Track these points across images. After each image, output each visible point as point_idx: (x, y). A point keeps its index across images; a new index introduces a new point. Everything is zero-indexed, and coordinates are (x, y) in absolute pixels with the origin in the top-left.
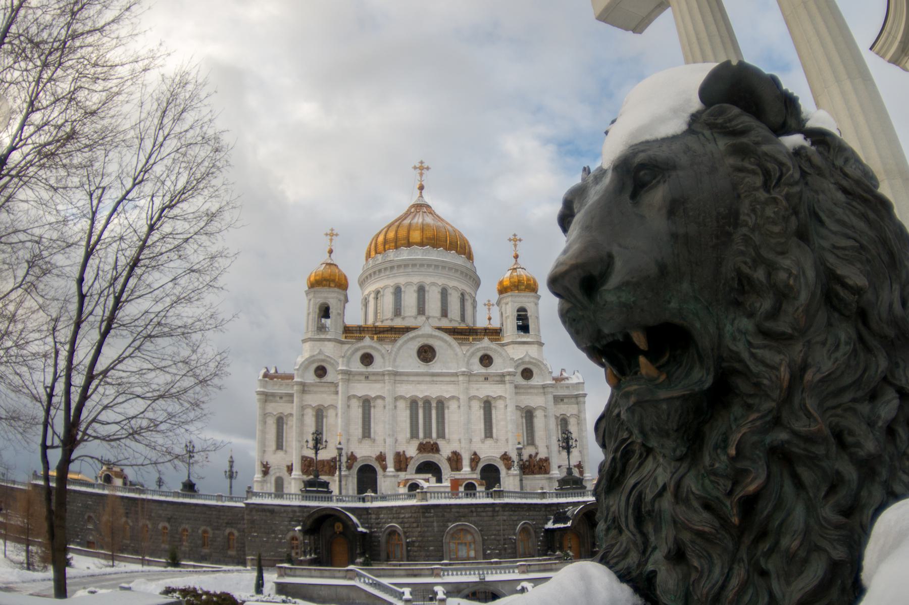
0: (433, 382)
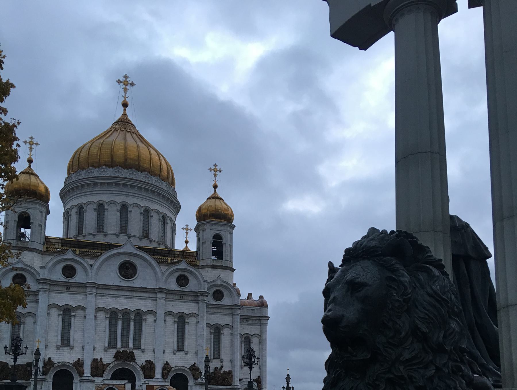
0: (132, 297)
